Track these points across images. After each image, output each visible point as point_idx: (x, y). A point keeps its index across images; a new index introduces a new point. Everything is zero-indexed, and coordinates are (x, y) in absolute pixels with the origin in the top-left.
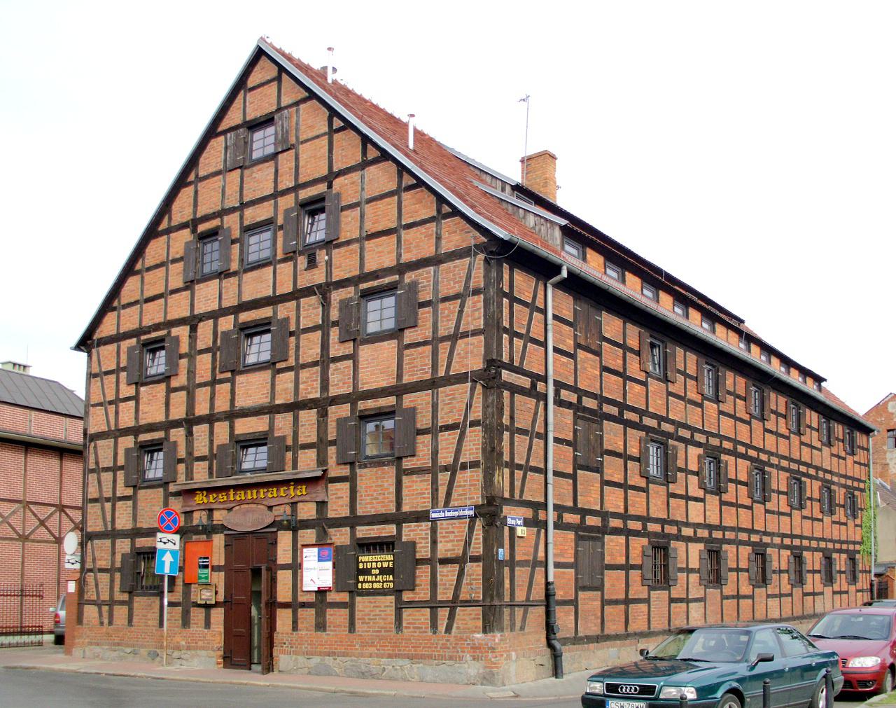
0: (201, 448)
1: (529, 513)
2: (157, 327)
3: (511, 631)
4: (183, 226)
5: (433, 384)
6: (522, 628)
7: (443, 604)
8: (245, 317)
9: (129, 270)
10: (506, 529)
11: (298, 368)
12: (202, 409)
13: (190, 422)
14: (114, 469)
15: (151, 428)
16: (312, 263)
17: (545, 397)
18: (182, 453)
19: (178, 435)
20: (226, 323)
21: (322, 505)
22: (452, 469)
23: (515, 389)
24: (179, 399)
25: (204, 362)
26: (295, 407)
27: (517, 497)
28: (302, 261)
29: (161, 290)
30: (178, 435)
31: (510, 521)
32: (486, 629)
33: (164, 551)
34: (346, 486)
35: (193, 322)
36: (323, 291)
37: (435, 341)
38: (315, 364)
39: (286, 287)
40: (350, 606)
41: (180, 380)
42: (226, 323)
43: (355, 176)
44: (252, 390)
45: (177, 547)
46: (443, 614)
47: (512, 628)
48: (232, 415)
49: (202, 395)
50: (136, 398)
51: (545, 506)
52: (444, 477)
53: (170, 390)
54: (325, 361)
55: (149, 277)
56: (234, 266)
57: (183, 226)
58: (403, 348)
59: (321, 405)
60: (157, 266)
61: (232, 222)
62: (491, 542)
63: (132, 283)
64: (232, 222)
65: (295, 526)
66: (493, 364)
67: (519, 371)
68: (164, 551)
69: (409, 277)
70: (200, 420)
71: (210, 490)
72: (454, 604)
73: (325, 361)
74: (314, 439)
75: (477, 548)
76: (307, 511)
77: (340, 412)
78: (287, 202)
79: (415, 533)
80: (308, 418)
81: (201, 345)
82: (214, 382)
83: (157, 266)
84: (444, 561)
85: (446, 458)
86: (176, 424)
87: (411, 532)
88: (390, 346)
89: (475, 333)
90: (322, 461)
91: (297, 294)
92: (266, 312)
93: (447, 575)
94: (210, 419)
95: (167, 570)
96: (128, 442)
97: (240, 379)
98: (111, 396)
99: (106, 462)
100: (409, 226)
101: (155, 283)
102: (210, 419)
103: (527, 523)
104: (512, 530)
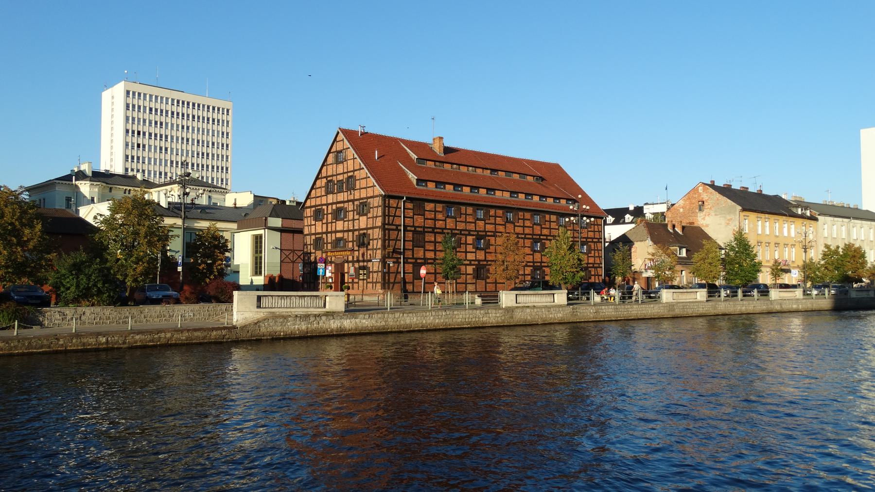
0: (329, 241)
1: (395, 260)
2: (319, 205)
4: (324, 177)
5: (373, 228)
6: (392, 289)
7: (374, 282)
8: (338, 205)
9: (312, 188)
11: (348, 221)
12: (329, 230)
13: (327, 233)
14: (311, 245)
15: (319, 234)
16: (351, 194)
18: (325, 241)
19: (324, 236)
20: (334, 207)
21: (353, 257)
22: (376, 249)
23: (389, 230)
24: (325, 226)
25: (330, 216)
26: (348, 231)
28: (349, 192)
29: (320, 195)
30: (324, 236)
32: (381, 289)
33: (320, 269)
34: (357, 252)
35: (327, 205)
36: (353, 201)
37: (373, 217)
38: (351, 220)
39: (346, 199)
40: (358, 283)
41: (325, 221)
42: (334, 207)
43: (358, 171)
44: (340, 225)
46: (374, 285)
48: (336, 232)
49: (329, 225)
50: (315, 225)
52: (375, 251)
53: (323, 224)
54: (354, 220)
55: (317, 190)
56: (336, 191)
57: (324, 177)
58: (368, 218)
59: (353, 231)
60: (319, 188)
61: (334, 178)
62: (384, 266)
63: (313, 191)
64: (334, 178)
65: (348, 262)
66: (384, 224)
67: (392, 224)
68: (320, 269)
69: (369, 200)
70: (329, 233)
71: (331, 252)
72: (376, 283)
73: (354, 220)
74: (351, 240)
75: (380, 270)
76: (350, 258)
77: (356, 233)
78: (346, 176)
79: (370, 264)
80: (350, 233)
81: (329, 212)
82: (332, 223)
83: (319, 188)
84: (375, 272)
85: (375, 247)
86: (324, 233)
87: (370, 264)
88: (365, 217)
89: (380, 216)
90: (353, 246)
91: (348, 201)
92: (342, 205)
93: (375, 275)
94: (331, 232)
95: (321, 274)
96: (313, 237)
97: (337, 222)
98: (309, 224)
99: (309, 243)
100: (368, 187)
101: (319, 192)
102: (331, 232)
103: (394, 262)
104: (389, 264)
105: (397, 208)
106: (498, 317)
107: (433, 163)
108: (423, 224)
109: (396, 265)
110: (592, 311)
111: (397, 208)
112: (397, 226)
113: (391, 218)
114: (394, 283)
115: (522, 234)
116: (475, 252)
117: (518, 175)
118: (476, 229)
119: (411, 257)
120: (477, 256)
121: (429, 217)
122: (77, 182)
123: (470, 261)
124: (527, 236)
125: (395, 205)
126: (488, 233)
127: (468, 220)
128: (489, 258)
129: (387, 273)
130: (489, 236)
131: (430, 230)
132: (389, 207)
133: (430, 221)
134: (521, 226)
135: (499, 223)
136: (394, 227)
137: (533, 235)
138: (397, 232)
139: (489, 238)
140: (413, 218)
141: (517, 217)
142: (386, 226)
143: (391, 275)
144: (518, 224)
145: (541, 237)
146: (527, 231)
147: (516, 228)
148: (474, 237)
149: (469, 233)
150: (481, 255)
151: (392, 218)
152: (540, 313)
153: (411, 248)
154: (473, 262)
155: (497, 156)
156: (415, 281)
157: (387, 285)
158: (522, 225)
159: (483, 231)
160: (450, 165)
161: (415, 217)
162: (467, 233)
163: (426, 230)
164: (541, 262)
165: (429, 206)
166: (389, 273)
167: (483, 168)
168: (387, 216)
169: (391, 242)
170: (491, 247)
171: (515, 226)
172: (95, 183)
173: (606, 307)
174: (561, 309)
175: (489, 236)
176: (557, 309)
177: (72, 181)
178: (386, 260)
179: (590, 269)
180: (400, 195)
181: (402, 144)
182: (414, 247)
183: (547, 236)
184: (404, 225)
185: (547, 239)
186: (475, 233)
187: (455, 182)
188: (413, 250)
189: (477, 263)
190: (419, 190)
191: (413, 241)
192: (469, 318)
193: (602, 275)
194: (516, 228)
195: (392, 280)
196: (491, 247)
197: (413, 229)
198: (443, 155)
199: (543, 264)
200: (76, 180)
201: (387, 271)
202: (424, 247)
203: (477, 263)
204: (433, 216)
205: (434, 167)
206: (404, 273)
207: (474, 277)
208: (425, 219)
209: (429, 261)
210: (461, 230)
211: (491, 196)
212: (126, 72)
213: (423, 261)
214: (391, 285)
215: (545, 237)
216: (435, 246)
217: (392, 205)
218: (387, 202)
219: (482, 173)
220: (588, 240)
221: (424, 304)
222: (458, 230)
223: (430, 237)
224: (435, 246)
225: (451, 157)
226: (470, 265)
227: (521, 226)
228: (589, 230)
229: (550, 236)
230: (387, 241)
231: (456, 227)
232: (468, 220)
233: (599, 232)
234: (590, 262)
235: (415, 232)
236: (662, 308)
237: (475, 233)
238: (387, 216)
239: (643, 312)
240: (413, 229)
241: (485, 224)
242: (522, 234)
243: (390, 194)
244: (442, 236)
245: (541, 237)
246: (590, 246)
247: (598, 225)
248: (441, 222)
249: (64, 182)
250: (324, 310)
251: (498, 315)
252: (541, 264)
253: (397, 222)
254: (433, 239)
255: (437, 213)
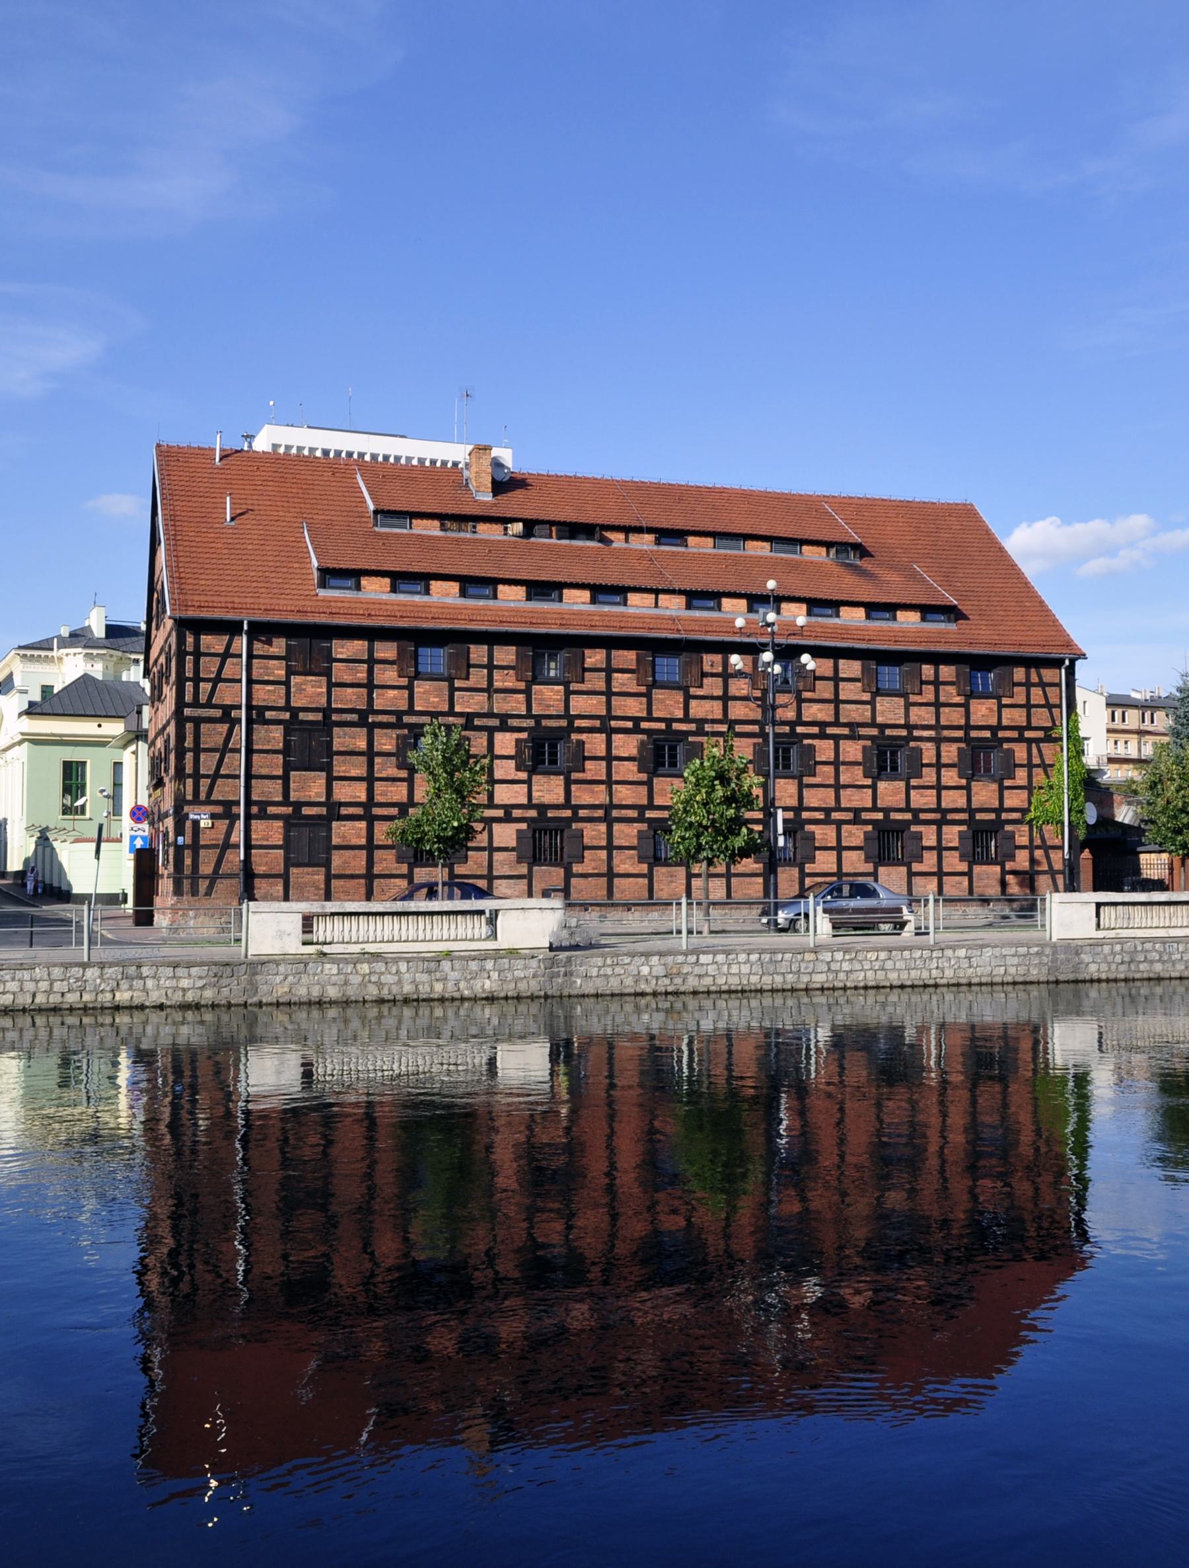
1: (219, 809)
3: (193, 895)
6: (208, 893)
10: (188, 824)
17: (239, 721)
23: (197, 721)
27: (203, 796)
31: (191, 816)
45: (146, 834)
47: (194, 892)
51: (238, 803)
62: (179, 831)
67: (209, 705)
103: (213, 816)
104: (196, 823)
105: (226, 655)
106: (184, 990)
107: (437, 523)
108: (324, 700)
109: (223, 825)
110: (645, 970)
111: (226, 655)
112: (227, 709)
113: (205, 687)
114: (215, 877)
115: (714, 721)
116: (529, 782)
117: (767, 545)
118: (529, 707)
119: (280, 798)
120: (534, 794)
121: (347, 678)
122: (62, 651)
123: (508, 808)
124: (738, 728)
125: (220, 649)
126: (578, 723)
127: (497, 684)
128: (581, 795)
129: (188, 847)
130: (581, 730)
131: (354, 717)
132: (197, 654)
133: (349, 690)
134: (713, 698)
135: (624, 689)
136: (218, 713)
137: (873, 724)
138: (226, 727)
139: (584, 737)
140: (287, 684)
141: (695, 670)
142: (187, 712)
143: (202, 852)
144: (700, 692)
145: (799, 730)
146: (738, 711)
147: (693, 703)
148: (524, 735)
149: (399, 719)
150: (549, 789)
151: (209, 686)
152: (388, 979)
153: (280, 772)
154: (516, 813)
155: (723, 491)
156: (293, 870)
157: (186, 884)
158: (720, 693)
159: (558, 717)
160: (498, 528)
161: (294, 680)
162: (495, 722)
163: (335, 717)
164: (1001, 809)
165: (344, 649)
166: (195, 847)
167: (628, 530)
168: (189, 679)
169: (203, 756)
170: (589, 765)
171: (688, 698)
172: (95, 652)
173: (720, 958)
174: (489, 964)
175: (581, 730)
176: (474, 965)
177: (52, 649)
178: (186, 809)
179: (1008, 828)
180: (230, 616)
181: (359, 477)
182: (288, 767)
183: (822, 725)
184: (250, 707)
185: (823, 736)
186: (531, 723)
187: (464, 571)
188: (286, 779)
189: (533, 813)
190: (325, 600)
191: (286, 751)
192: (49, 992)
193: (1061, 848)
194: (693, 703)
195: (206, 869)
196: (589, 765)
197: (287, 716)
198: (488, 497)
199: (1004, 816)
200: (59, 648)
201: (189, 841)
202: (328, 768)
203: (533, 813)
204: (362, 676)
205: (438, 533)
206: (248, 847)
207: (520, 860)
208: (331, 685)
209: (344, 811)
210: (469, 717)
211: (606, 608)
212: (271, 403)
213: (323, 811)
214: (203, 885)
215: (815, 730)
216: (371, 765)
217: (208, 647)
218: (190, 639)
219: (625, 545)
220: (1001, 734)
221: (699, 929)
222: (461, 715)
223: (349, 739)
224: (371, 765)
225: (513, 503)
226: (508, 819)
227: (713, 698)
228: (1005, 701)
229: (836, 723)
230: (189, 756)
231: (452, 705)
232: (497, 684)
233: (1049, 706)
234: (1008, 803)
235: (292, 726)
236: (1015, 961)
237: (531, 723)
238: (189, 679)
239: (913, 974)
240: (287, 716)
241: (568, 693)
242: (714, 721)
243: (191, 614)
244: (394, 733)
245: (799, 730)
246: (920, 751)
247: (1043, 685)
248: (392, 693)
249: (36, 653)
250: (490, 945)
251: (185, 983)
252: (998, 816)
253: (227, 695)
254: (362, 745)
255: (377, 667)
